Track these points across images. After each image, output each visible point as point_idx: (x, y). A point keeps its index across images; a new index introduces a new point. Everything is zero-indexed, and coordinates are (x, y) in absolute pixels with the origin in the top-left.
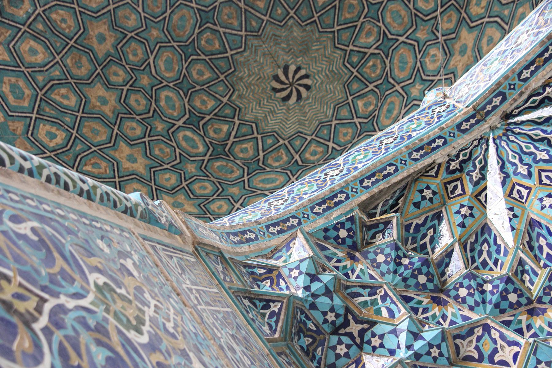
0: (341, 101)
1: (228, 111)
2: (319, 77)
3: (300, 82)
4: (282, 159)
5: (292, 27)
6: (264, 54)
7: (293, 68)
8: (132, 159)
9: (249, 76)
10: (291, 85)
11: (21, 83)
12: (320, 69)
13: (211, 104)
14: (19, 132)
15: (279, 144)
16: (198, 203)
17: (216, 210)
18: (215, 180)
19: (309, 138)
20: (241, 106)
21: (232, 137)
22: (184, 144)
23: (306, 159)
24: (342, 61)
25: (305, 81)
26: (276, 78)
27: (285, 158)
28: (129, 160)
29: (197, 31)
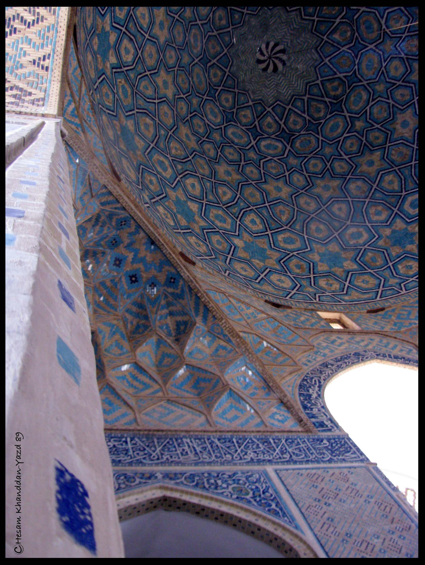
0: (318, 44)
1: (259, 108)
2: (287, 39)
3: (274, 51)
4: (320, 108)
5: (249, 20)
6: (243, 53)
7: (263, 46)
8: (279, 189)
9: (245, 74)
10: (270, 58)
11: (215, 212)
12: (284, 33)
13: (248, 113)
14: (251, 239)
15: (306, 100)
16: (330, 177)
17: (344, 171)
18: (312, 155)
19: (319, 82)
20: (260, 98)
21: (280, 122)
22: (271, 152)
23: (334, 96)
24: (299, 18)
25: (278, 48)
26: (259, 62)
27: (322, 106)
28: (279, 192)
29: (207, 76)
